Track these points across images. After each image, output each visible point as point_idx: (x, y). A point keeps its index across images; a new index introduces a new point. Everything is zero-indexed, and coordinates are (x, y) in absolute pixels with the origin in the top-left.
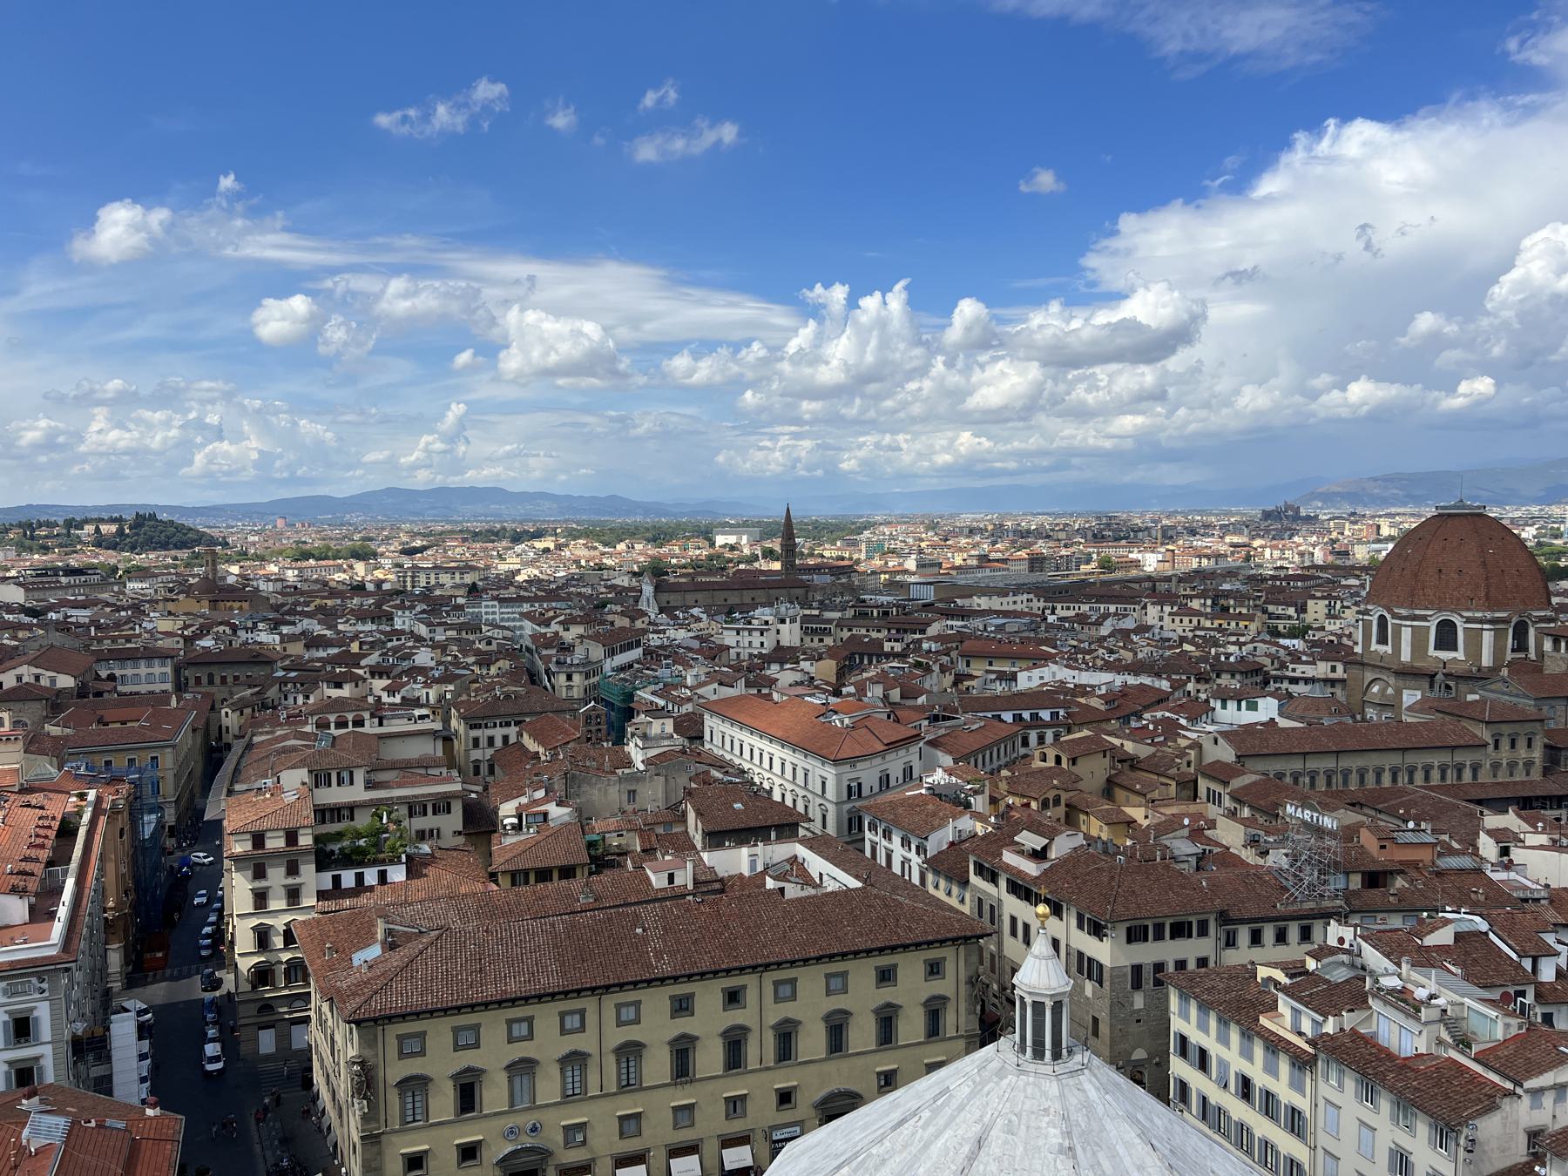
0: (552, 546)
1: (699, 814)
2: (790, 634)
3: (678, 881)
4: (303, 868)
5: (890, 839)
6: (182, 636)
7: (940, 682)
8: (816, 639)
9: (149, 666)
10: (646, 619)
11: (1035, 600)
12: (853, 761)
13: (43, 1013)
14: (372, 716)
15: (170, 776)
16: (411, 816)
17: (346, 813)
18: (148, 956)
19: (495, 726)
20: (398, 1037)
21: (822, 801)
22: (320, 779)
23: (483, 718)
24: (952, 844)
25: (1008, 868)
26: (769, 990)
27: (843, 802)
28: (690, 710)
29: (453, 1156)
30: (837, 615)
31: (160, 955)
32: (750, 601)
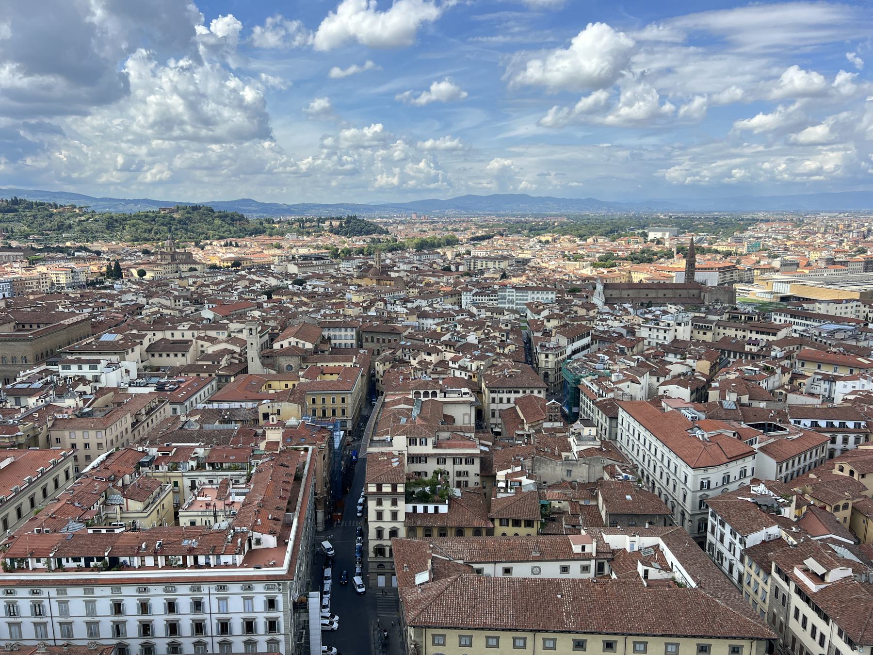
0: (550, 240)
1: (605, 500)
2: (684, 333)
3: (587, 550)
4: (399, 503)
5: (724, 527)
6: (362, 306)
7: (781, 379)
8: (701, 332)
9: (346, 331)
10: (596, 310)
11: (862, 306)
12: (705, 468)
13: (280, 598)
14: (441, 392)
15: (350, 407)
16: (454, 464)
17: (423, 459)
18: (334, 514)
19: (503, 392)
20: (432, 635)
21: (684, 487)
22: (412, 441)
23: (497, 388)
24: (764, 542)
25: (797, 580)
26: (630, 646)
27: (697, 491)
28: (612, 397)
30: (716, 318)
32: (663, 296)
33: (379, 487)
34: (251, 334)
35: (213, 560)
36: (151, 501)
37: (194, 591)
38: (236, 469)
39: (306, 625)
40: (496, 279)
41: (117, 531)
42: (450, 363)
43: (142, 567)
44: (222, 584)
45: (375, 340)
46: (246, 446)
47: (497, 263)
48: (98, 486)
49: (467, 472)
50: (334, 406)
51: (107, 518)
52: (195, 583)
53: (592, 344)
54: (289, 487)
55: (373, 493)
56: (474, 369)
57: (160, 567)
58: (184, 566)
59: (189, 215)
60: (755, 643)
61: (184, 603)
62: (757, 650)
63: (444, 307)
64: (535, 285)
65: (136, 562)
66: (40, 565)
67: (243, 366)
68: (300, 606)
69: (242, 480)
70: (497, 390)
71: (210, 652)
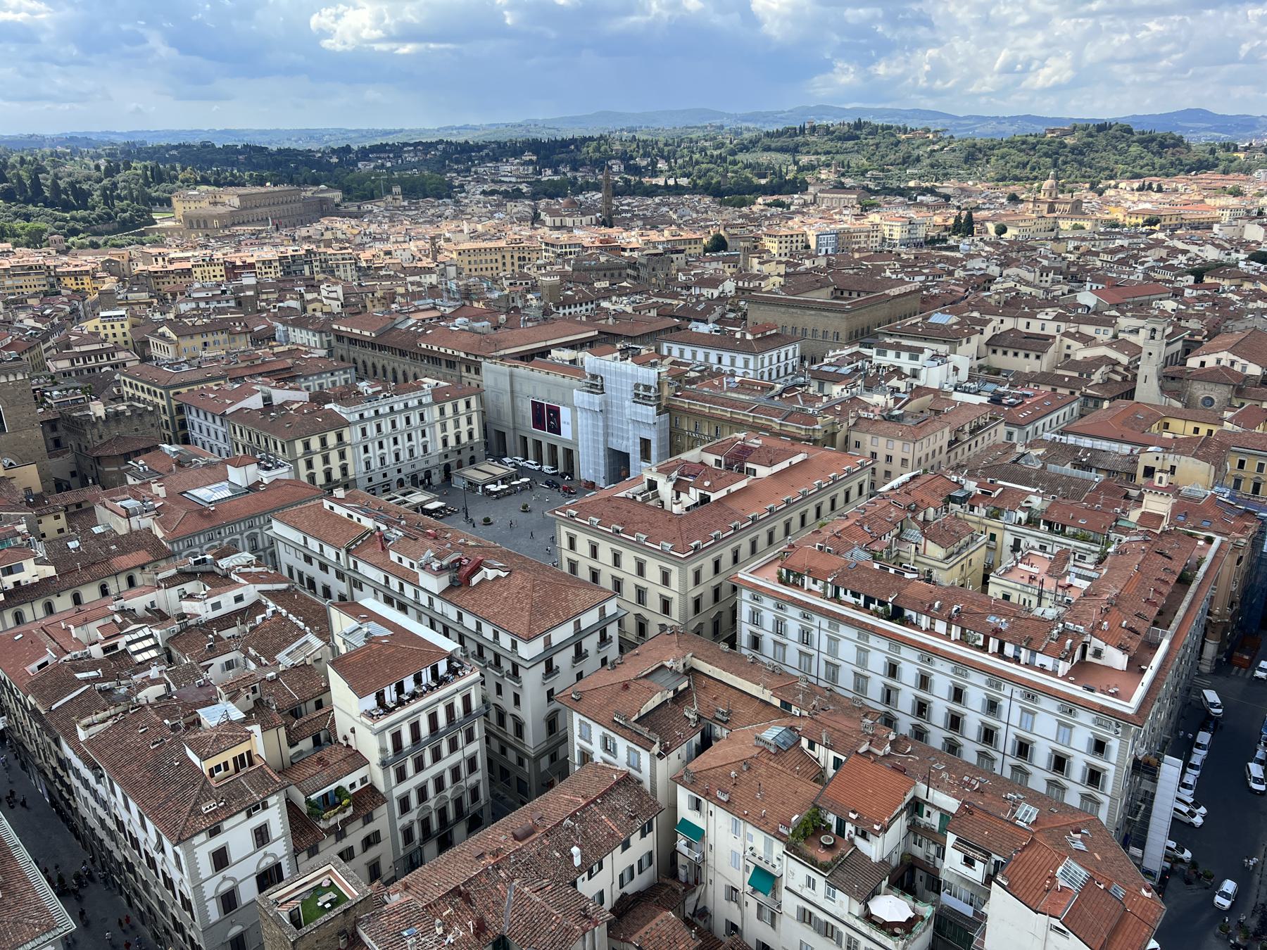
13: (1114, 744)
18: (1237, 654)
31: (1247, 658)
34: (1153, 338)
35: (1024, 655)
36: (956, 551)
38: (1084, 539)
39: (1149, 798)
41: (908, 576)
43: (930, 631)
44: (1032, 692)
46: (1107, 510)
48: (894, 513)
51: (897, 555)
52: (997, 677)
54: (1166, 590)
57: (953, 639)
58: (984, 648)
59: (1090, 139)
61: (976, 696)
65: (924, 621)
66: (816, 588)
67: (1127, 387)
68: (1145, 769)
69: (1091, 558)
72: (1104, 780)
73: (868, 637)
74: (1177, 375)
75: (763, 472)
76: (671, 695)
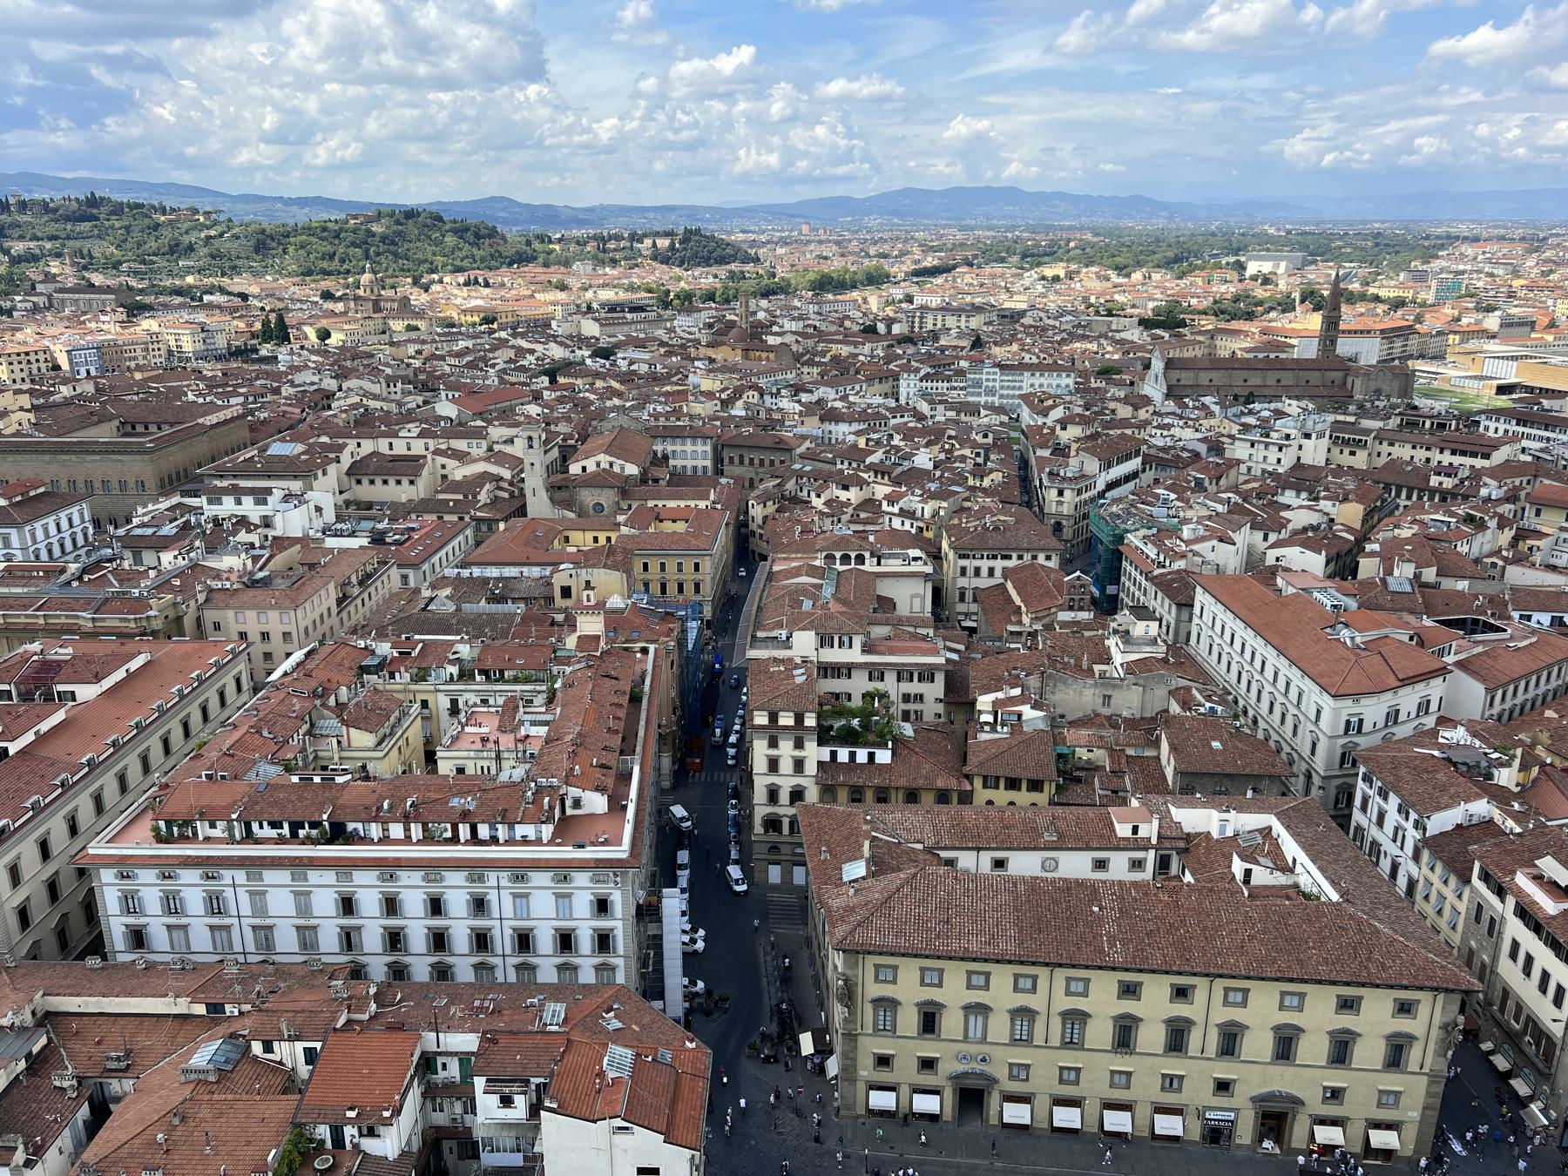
0: (1062, 275)
1: (1173, 748)
2: (1315, 452)
3: (1142, 833)
4: (807, 744)
5: (1386, 799)
6: (719, 399)
7: (1495, 538)
8: (1346, 451)
9: (694, 444)
10: (1151, 409)
12: (1356, 696)
13: (616, 897)
14: (872, 555)
15: (708, 578)
16: (899, 681)
17: (845, 671)
18: (689, 760)
19: (982, 557)
21: (1313, 728)
22: (825, 641)
24: (1459, 826)
25: (1519, 893)
26: (1218, 994)
27: (1339, 737)
28: (1183, 567)
29: (915, 1064)
30: (1376, 424)
32: (1274, 383)
33: (773, 717)
35: (502, 832)
36: (388, 732)
37: (473, 881)
38: (527, 681)
39: (656, 942)
40: (963, 348)
41: (339, 780)
42: (885, 503)
43: (385, 840)
44: (519, 872)
45: (747, 461)
46: (542, 642)
47: (963, 318)
48: (297, 705)
49: (921, 696)
50: (682, 577)
51: (316, 757)
52: (477, 869)
53: (1144, 470)
54: (622, 713)
55: (763, 727)
56: (927, 515)
57: (414, 840)
58: (455, 840)
60: (1441, 997)
61: (457, 901)
62: (1443, 1008)
63: (869, 401)
64: (1035, 360)
65: (375, 830)
66: (217, 833)
67: (517, 504)
68: (648, 913)
69: (540, 700)
70: (971, 554)
71: (501, 979)
72: (614, 941)
73: (306, 875)
74: (563, 483)
75: (86, 692)
76: (22, 1065)
